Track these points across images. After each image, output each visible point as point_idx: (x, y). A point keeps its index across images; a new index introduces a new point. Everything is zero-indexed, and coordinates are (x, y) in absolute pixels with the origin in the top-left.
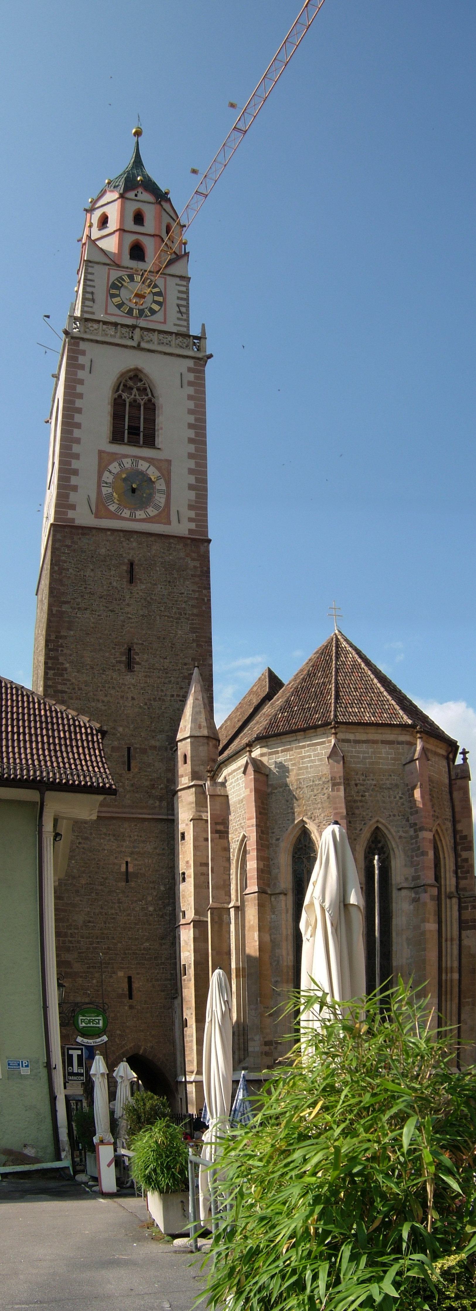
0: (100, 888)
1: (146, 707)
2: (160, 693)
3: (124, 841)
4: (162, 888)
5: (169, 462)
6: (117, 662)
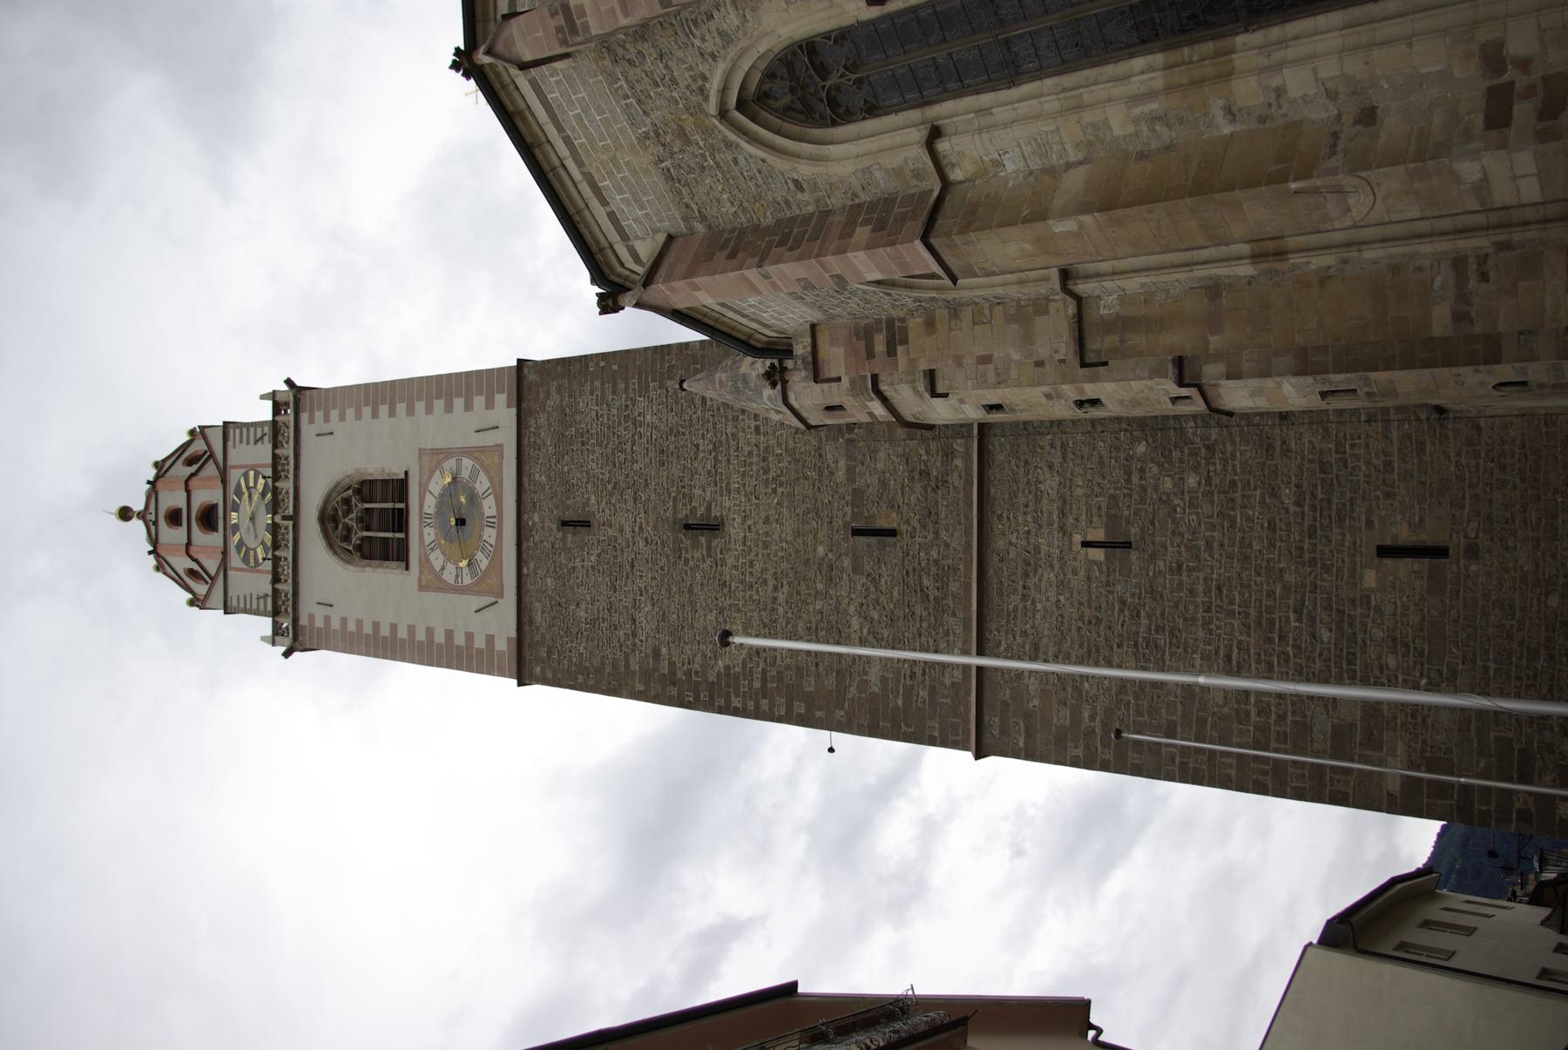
0: (1144, 621)
1: (780, 490)
2: (755, 459)
3: (1037, 549)
4: (1141, 448)
5: (421, 452)
6: (709, 555)
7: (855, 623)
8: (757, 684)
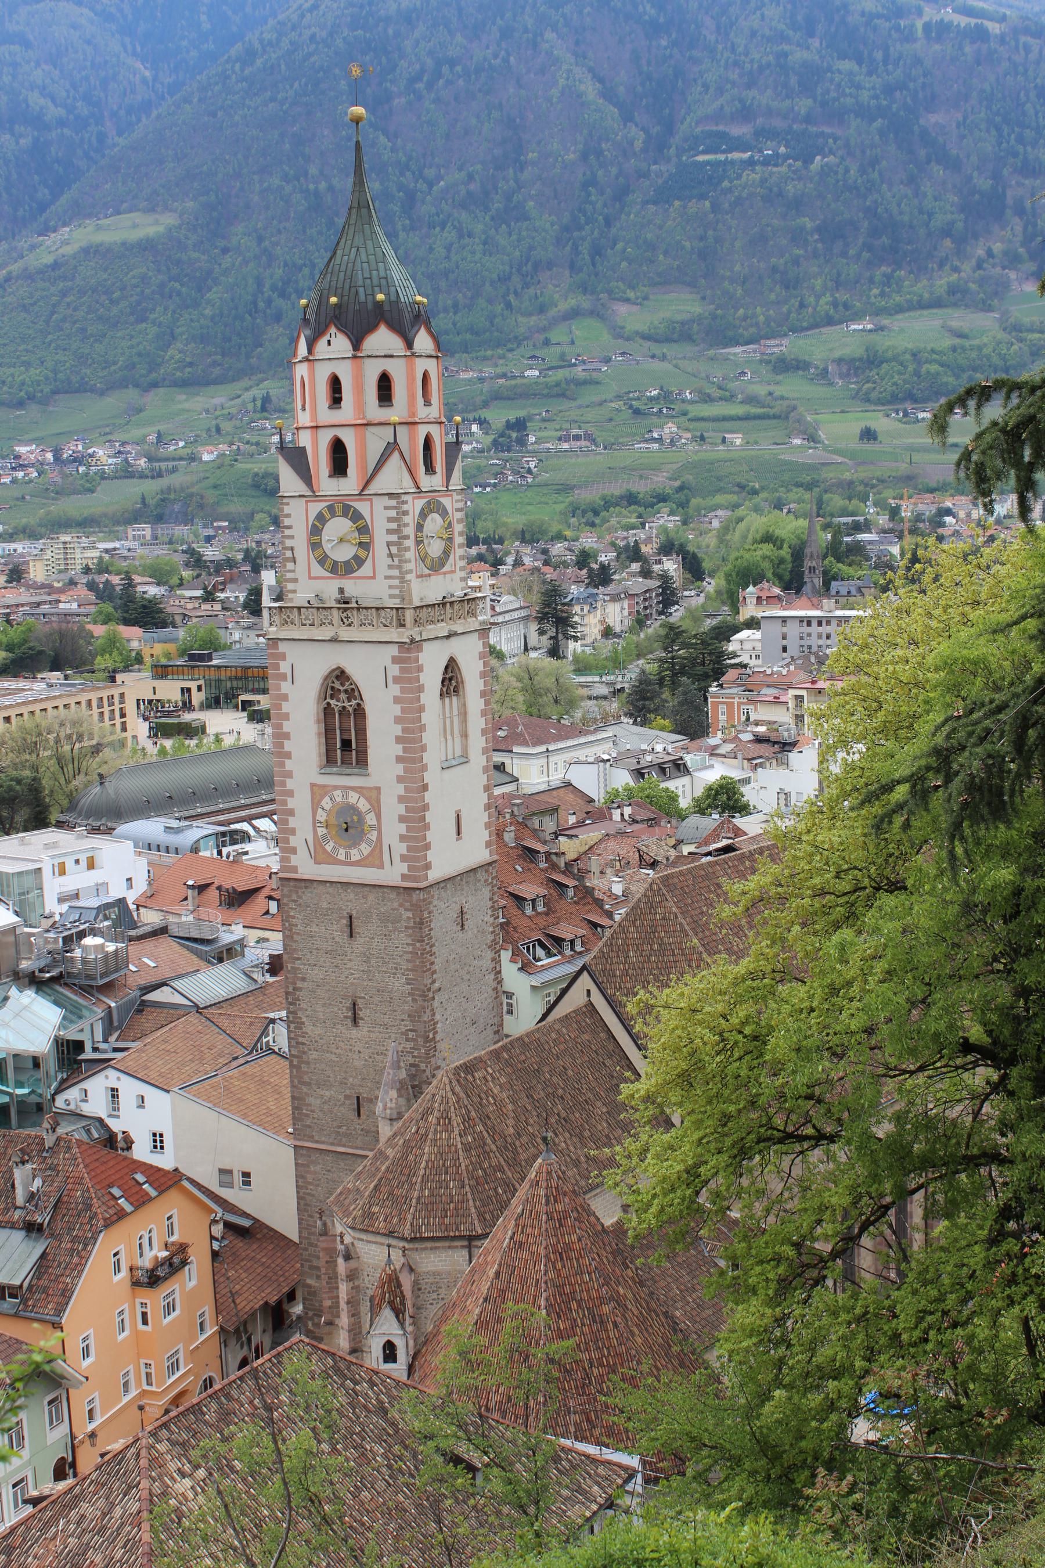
5: (378, 789)
7: (327, 1093)
8: (301, 1040)
